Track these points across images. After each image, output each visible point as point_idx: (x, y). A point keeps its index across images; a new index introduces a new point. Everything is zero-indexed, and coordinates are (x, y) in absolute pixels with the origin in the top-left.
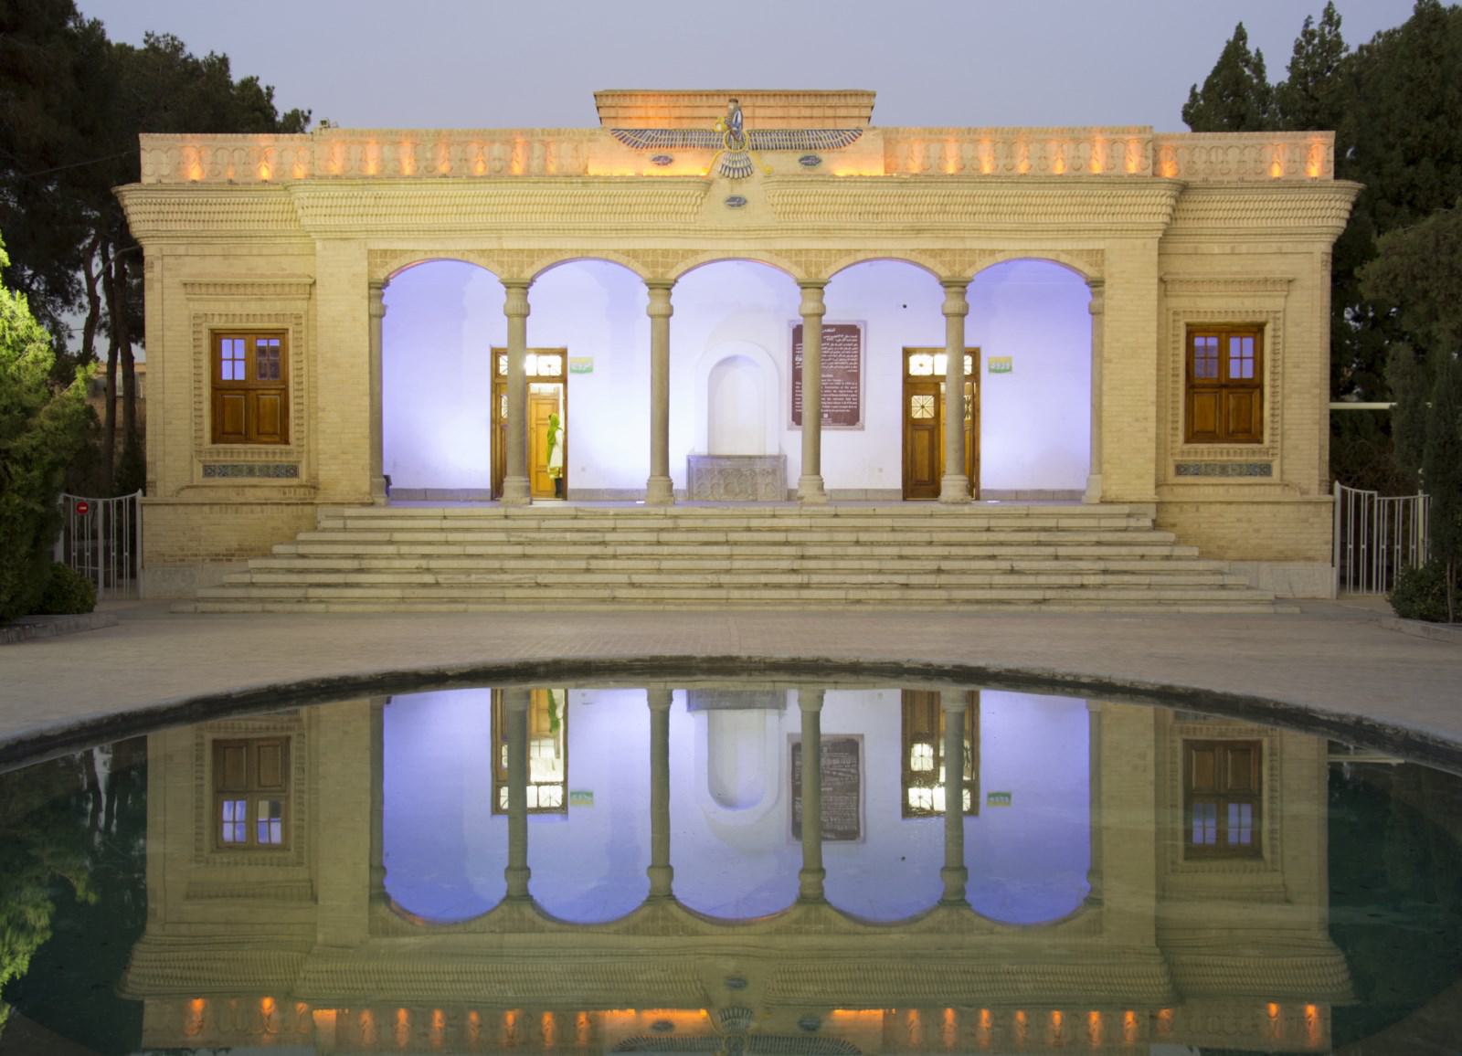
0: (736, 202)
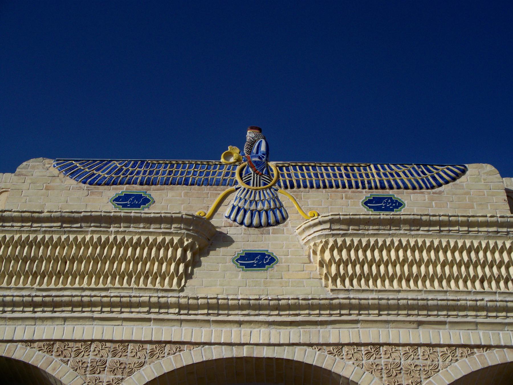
0: (256, 261)
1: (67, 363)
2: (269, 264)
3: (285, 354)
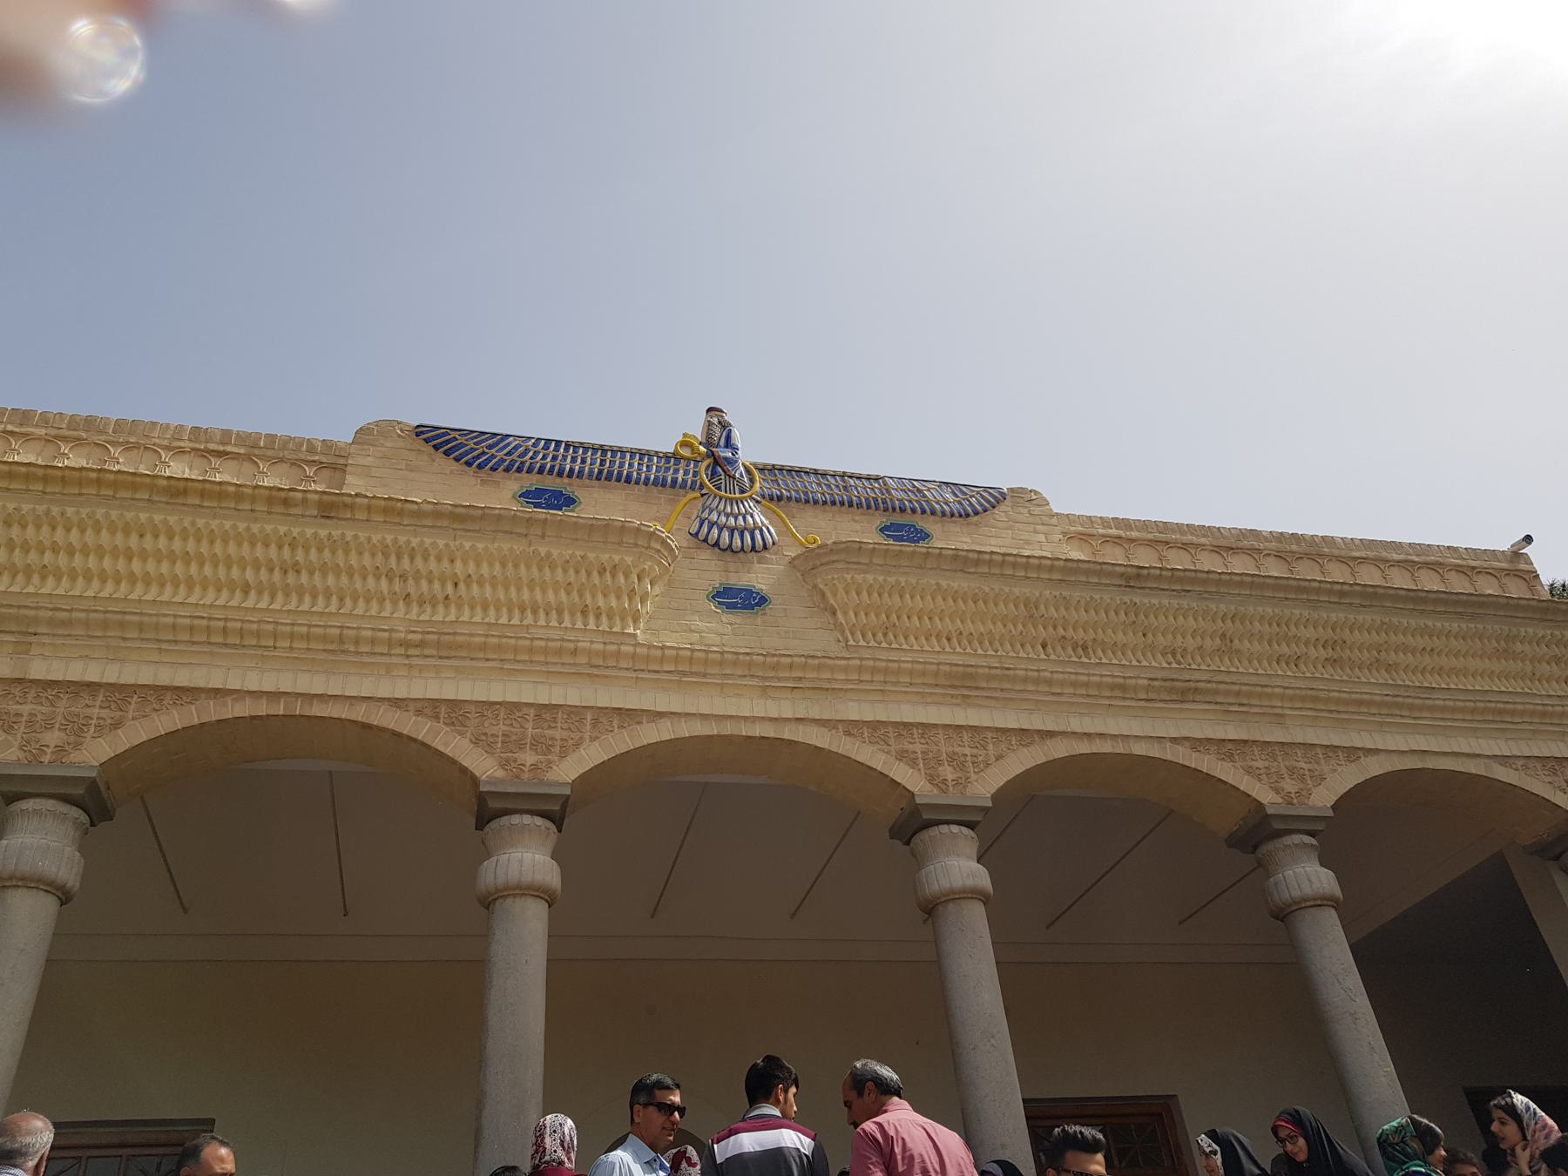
1: (461, 734)
2: (759, 604)
3: (787, 733)
